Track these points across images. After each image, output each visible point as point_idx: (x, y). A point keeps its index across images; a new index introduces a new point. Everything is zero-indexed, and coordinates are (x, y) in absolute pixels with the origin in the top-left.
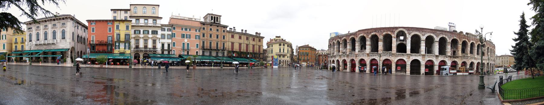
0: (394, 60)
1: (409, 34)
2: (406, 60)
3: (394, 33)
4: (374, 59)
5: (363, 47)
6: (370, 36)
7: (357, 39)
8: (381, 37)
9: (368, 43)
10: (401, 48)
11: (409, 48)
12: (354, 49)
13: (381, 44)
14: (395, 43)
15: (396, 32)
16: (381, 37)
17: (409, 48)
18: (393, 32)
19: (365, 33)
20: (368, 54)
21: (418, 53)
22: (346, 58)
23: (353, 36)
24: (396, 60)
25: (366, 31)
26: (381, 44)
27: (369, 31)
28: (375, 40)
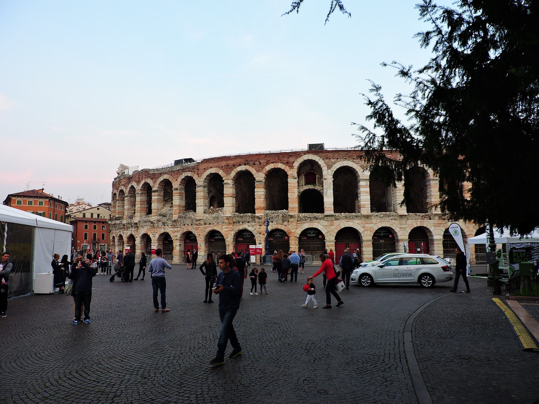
0: (295, 230)
1: (329, 167)
2: (324, 231)
3: (291, 167)
4: (245, 230)
5: (216, 200)
6: (233, 174)
7: (200, 181)
8: (260, 176)
9: (229, 190)
10: (311, 202)
11: (329, 200)
12: (191, 205)
13: (260, 193)
14: (296, 190)
15: (296, 164)
16: (260, 176)
17: (329, 200)
18: (290, 165)
19: (221, 168)
20: (228, 218)
21: (353, 211)
22: (168, 230)
23: (189, 174)
24: (299, 231)
25: (223, 163)
26: (260, 193)
27: (231, 163)
28: (245, 181)
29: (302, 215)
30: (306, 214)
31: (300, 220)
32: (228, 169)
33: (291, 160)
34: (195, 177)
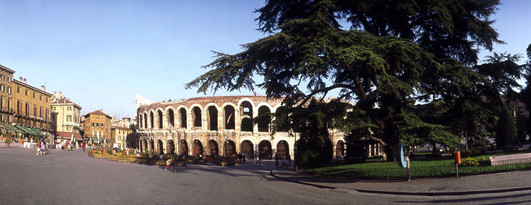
3: (237, 105)
5: (198, 123)
6: (206, 107)
12: (184, 124)
15: (240, 103)
18: (236, 103)
25: (201, 101)
27: (205, 101)
29: (242, 132)
30: (244, 132)
31: (241, 135)
32: (204, 104)
33: (237, 100)
34: (186, 108)
